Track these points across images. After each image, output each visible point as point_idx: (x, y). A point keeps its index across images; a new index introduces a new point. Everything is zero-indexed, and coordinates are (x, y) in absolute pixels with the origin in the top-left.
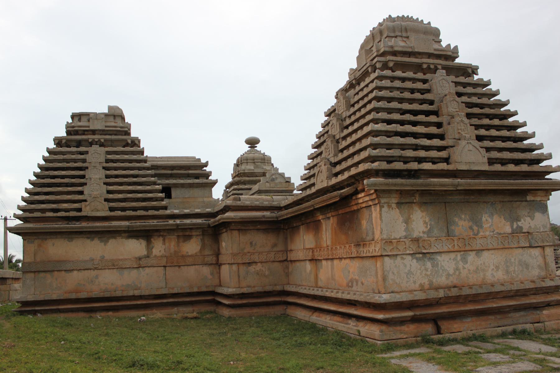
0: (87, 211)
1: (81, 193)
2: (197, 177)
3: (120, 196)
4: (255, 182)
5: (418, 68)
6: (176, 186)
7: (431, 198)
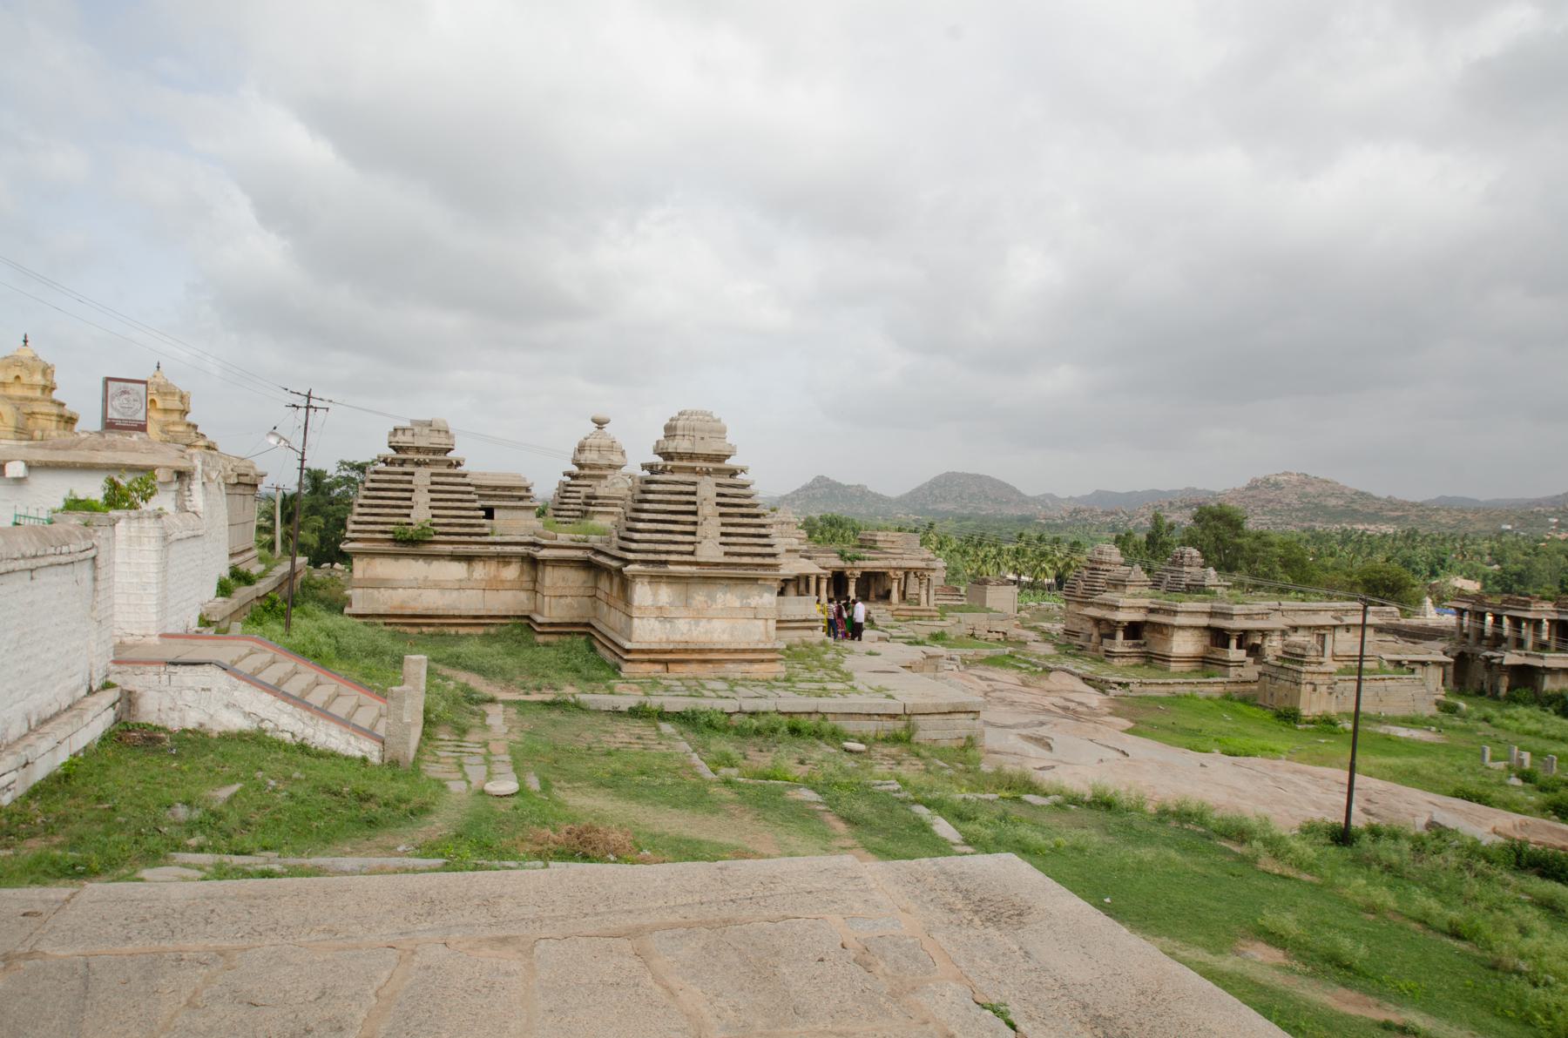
2: (521, 498)
5: (693, 470)
6: (499, 507)
7: (674, 579)
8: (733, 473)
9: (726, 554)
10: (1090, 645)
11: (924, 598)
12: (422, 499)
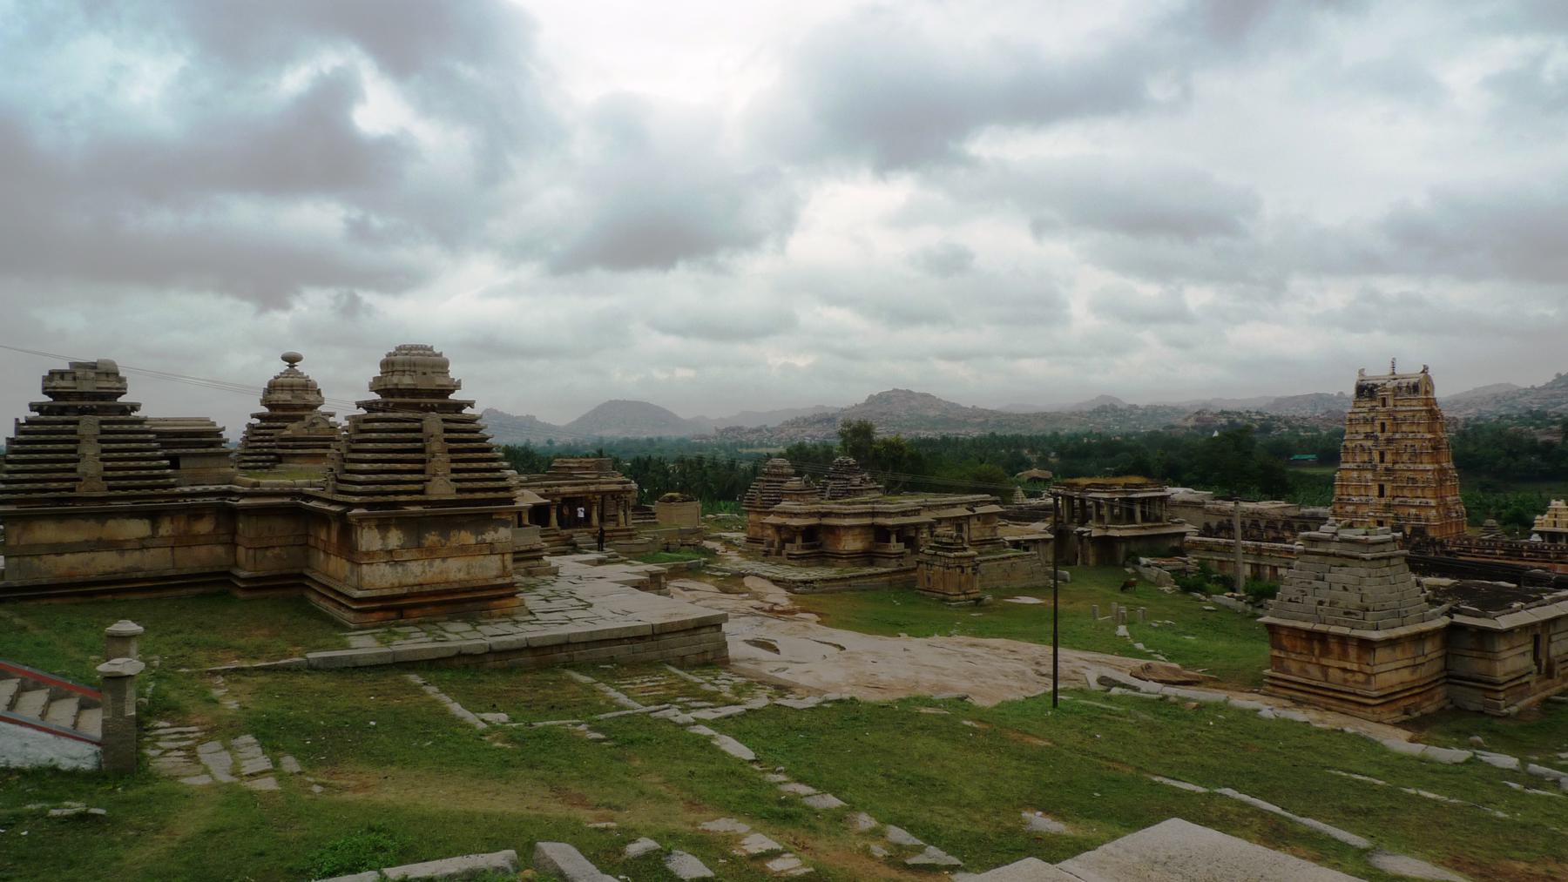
0: (82, 491)
1: (73, 470)
2: (211, 445)
3: (121, 473)
4: (294, 419)
5: (416, 407)
6: (185, 455)
7: (406, 523)
8: (459, 406)
9: (459, 491)
10: (773, 550)
11: (622, 519)
12: (90, 450)
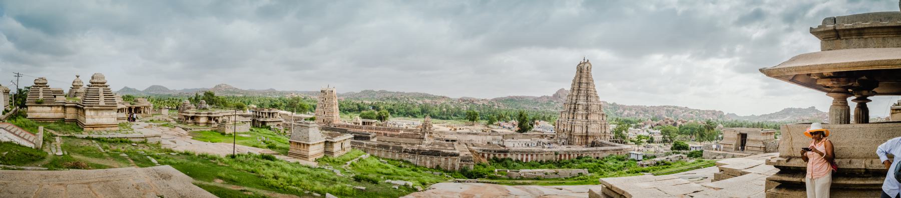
12: (41, 94)
